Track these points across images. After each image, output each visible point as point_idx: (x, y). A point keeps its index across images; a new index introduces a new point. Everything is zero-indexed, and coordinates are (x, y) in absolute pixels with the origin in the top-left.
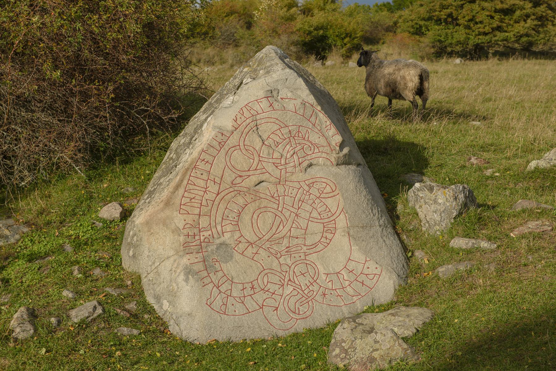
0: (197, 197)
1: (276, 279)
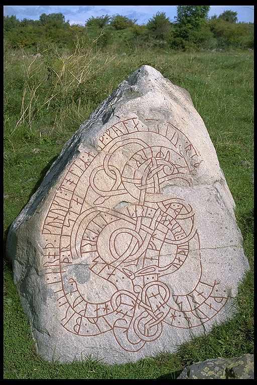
0: (61, 217)
1: (128, 301)
